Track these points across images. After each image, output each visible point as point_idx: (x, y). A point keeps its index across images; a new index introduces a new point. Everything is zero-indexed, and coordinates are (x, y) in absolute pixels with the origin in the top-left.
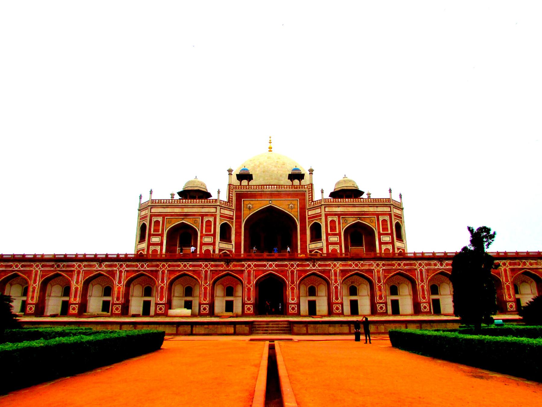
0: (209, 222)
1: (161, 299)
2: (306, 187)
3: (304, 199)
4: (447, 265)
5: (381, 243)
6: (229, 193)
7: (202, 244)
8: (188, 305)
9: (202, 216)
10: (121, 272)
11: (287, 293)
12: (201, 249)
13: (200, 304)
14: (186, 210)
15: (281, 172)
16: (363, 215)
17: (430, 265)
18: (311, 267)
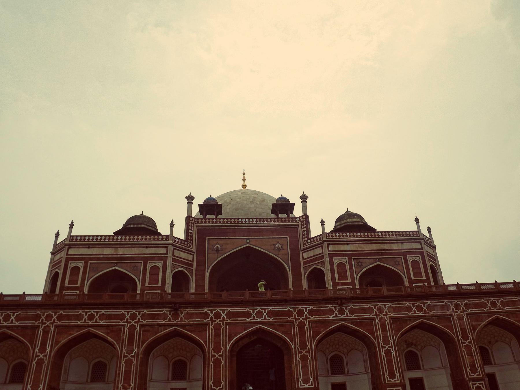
0: (155, 269)
2: (298, 219)
9: (146, 259)
14: (121, 251)
15: (260, 210)
16: (383, 254)
18: (336, 316)
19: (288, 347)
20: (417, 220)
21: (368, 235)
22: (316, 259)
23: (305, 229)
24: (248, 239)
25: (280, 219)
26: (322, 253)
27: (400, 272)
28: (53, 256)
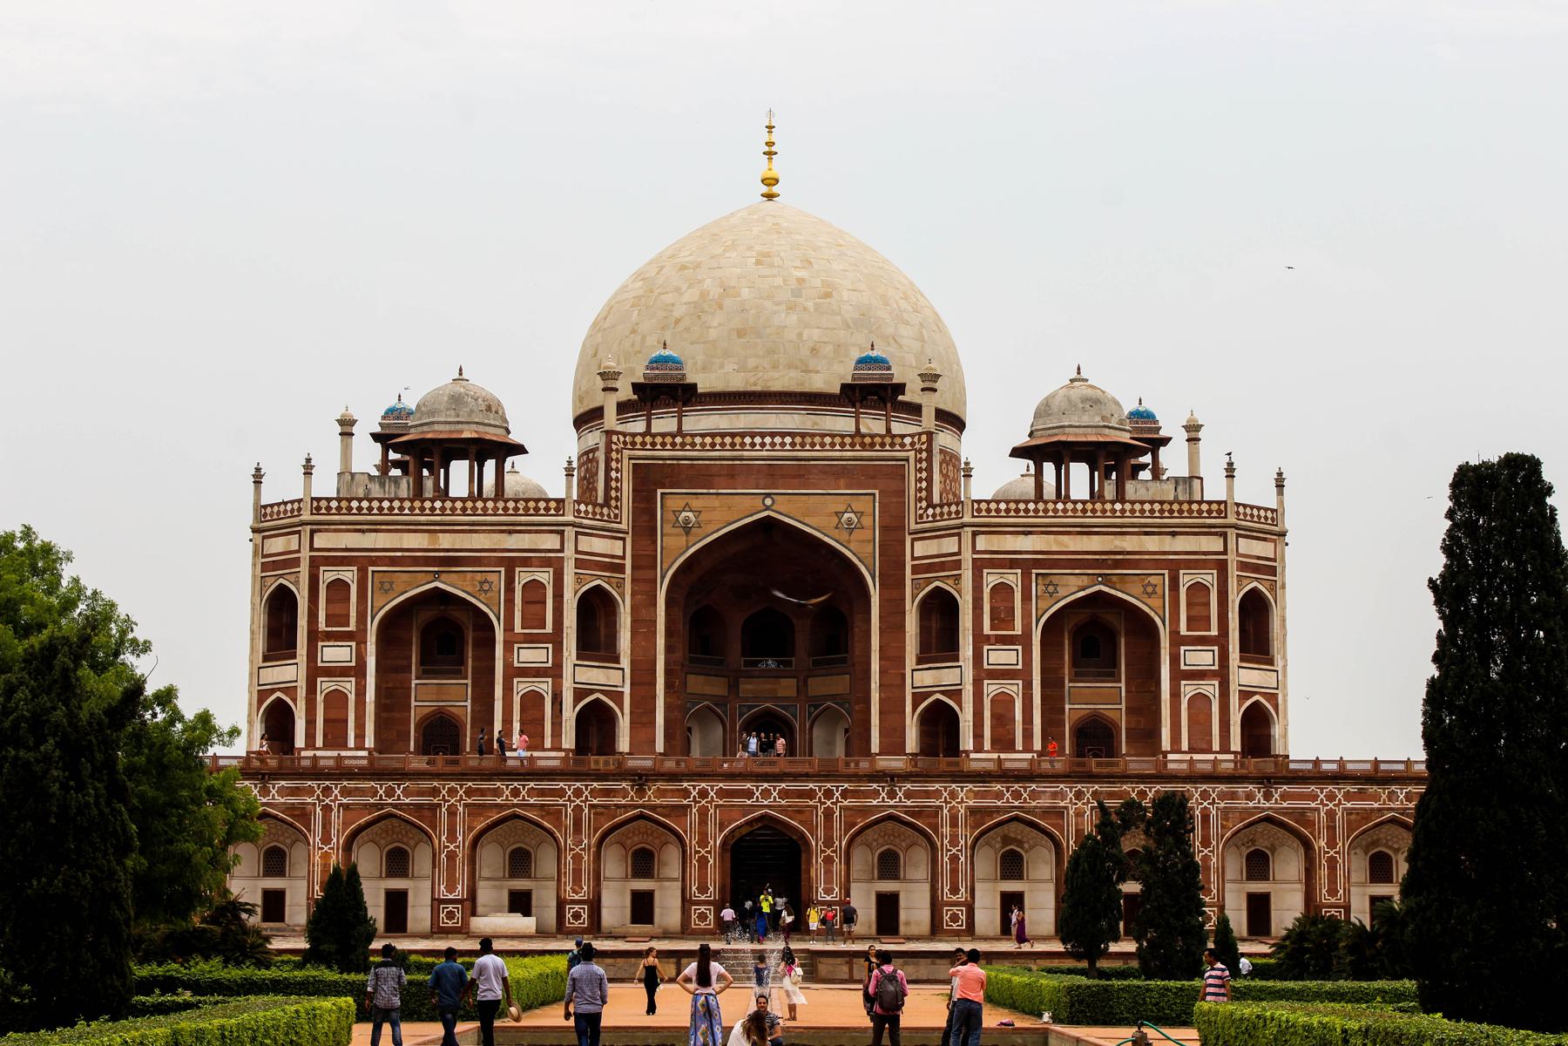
0: (534, 587)
1: (451, 888)
3: (901, 493)
4: (1284, 797)
5: (1178, 675)
6: (608, 469)
7: (512, 672)
8: (520, 903)
9: (510, 564)
10: (327, 809)
11: (813, 873)
12: (508, 689)
13: (561, 904)
14: (446, 541)
15: (816, 334)
16: (1117, 564)
17: (1233, 796)
18: (882, 800)
19: (807, 843)
20: (1230, 471)
21: (1084, 511)
22: (942, 567)
23: (924, 475)
24: (768, 495)
25: (858, 440)
26: (959, 553)
27: (1152, 614)
28: (259, 537)
